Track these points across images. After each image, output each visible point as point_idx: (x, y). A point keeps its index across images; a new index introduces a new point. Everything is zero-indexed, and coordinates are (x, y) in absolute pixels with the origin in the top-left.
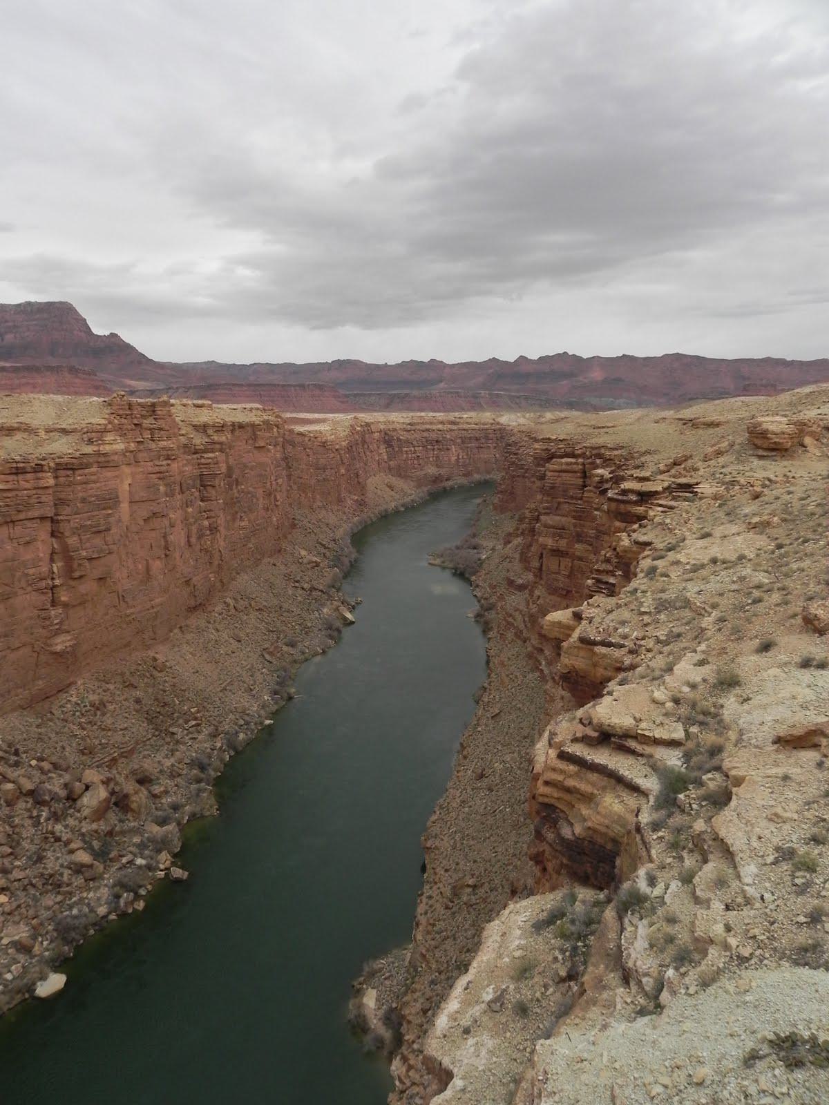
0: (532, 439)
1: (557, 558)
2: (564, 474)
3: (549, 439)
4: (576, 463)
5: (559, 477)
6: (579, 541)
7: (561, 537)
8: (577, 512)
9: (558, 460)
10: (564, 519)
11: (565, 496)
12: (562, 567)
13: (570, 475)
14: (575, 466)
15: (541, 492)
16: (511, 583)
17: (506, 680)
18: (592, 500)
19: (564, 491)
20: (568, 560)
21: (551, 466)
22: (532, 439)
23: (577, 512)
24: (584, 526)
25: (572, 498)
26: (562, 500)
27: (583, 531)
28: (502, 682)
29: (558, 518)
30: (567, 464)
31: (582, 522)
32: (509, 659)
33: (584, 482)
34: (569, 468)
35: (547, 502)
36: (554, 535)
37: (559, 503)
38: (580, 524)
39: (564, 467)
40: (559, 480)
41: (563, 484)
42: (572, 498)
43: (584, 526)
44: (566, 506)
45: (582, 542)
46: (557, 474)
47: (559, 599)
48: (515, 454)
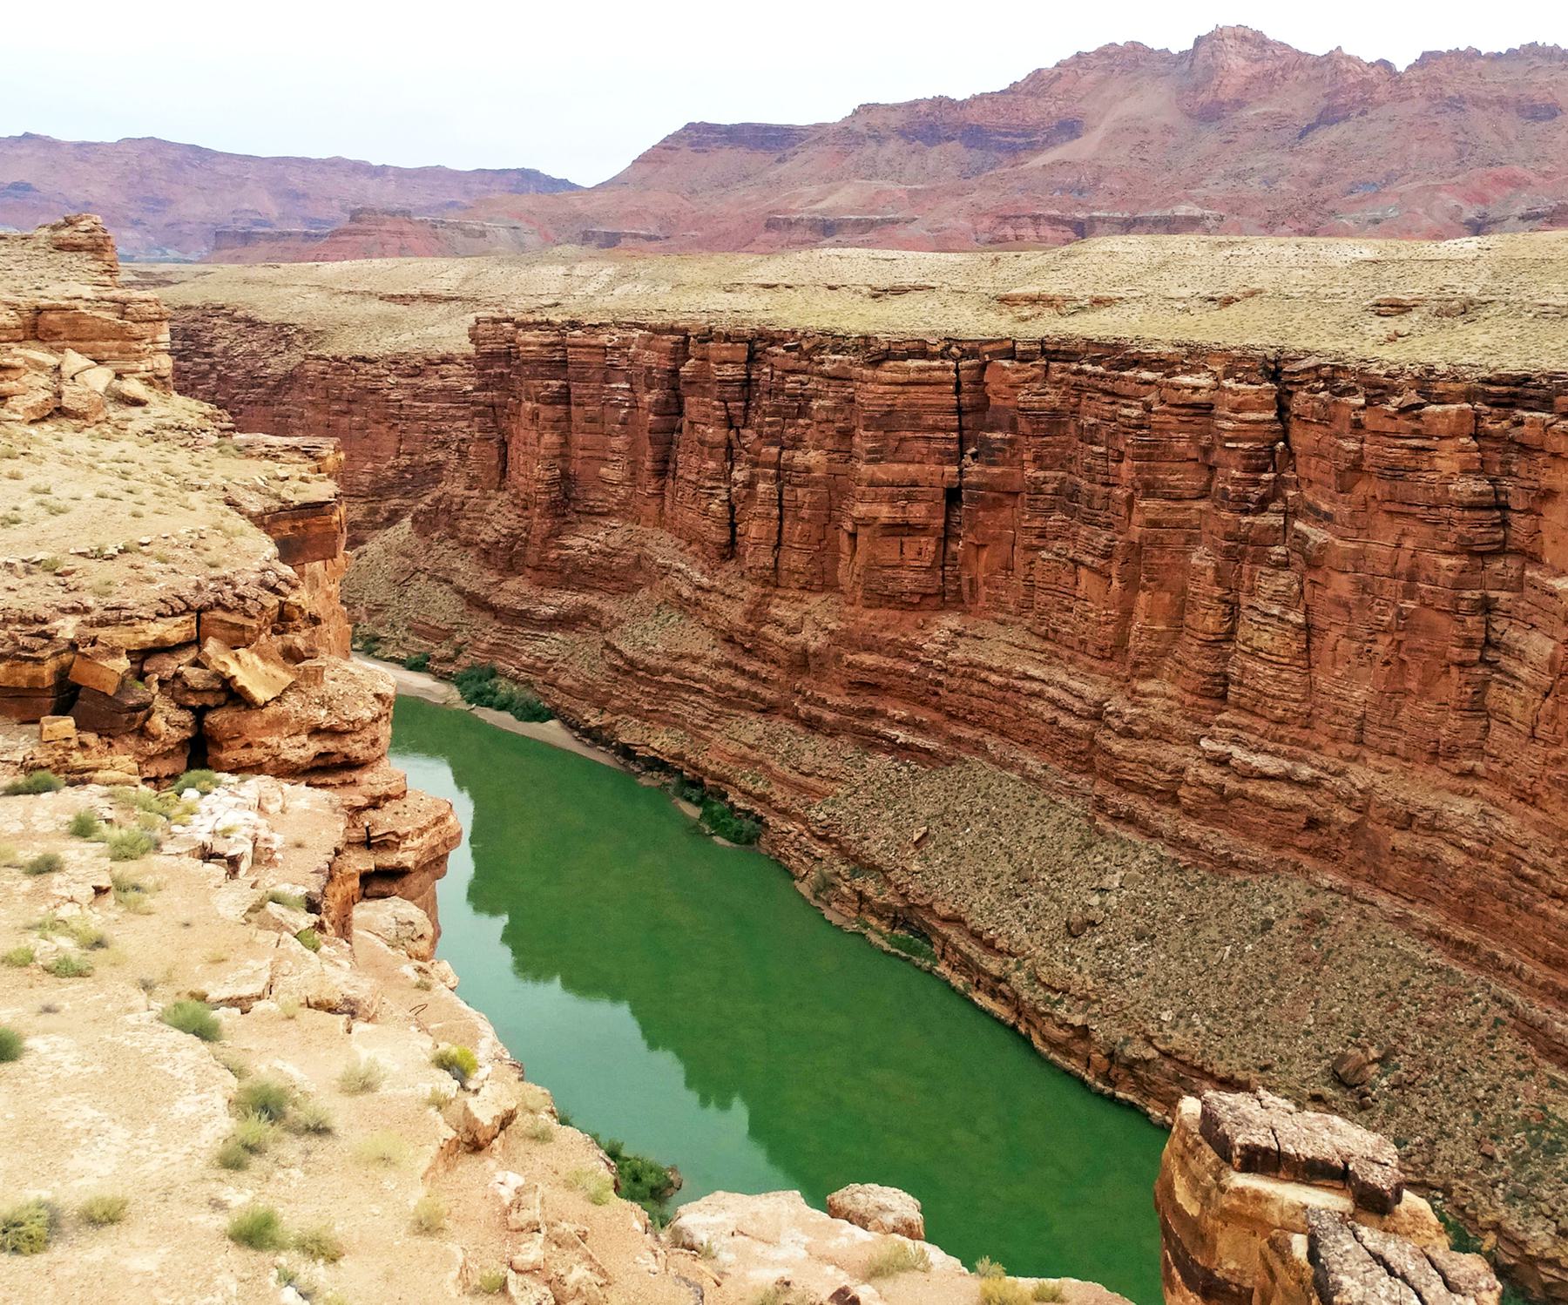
0: (238, 321)
1: (898, 539)
2: (912, 389)
3: (548, 323)
4: (947, 369)
5: (903, 393)
6: (1147, 496)
7: (910, 498)
8: (1143, 447)
9: (900, 363)
10: (911, 468)
11: (915, 427)
12: (910, 553)
13: (927, 388)
14: (938, 373)
15: (552, 427)
16: (520, 618)
17: (812, 781)
18: (1168, 426)
19: (912, 418)
20: (923, 539)
21: (883, 374)
22: (238, 321)
23: (1143, 447)
24: (1156, 469)
25: (935, 428)
26: (909, 434)
27: (1156, 479)
28: (801, 788)
29: (896, 467)
30: (920, 370)
31: (1152, 464)
32: (751, 747)
33: (958, 400)
34: (925, 376)
35: (875, 440)
36: (892, 500)
37: (902, 440)
38: (1149, 468)
39: (914, 375)
40: (901, 399)
41: (910, 405)
42: (935, 428)
43: (1156, 469)
44: (920, 445)
45: (1154, 496)
46: (900, 388)
47: (898, 613)
48: (207, 355)
